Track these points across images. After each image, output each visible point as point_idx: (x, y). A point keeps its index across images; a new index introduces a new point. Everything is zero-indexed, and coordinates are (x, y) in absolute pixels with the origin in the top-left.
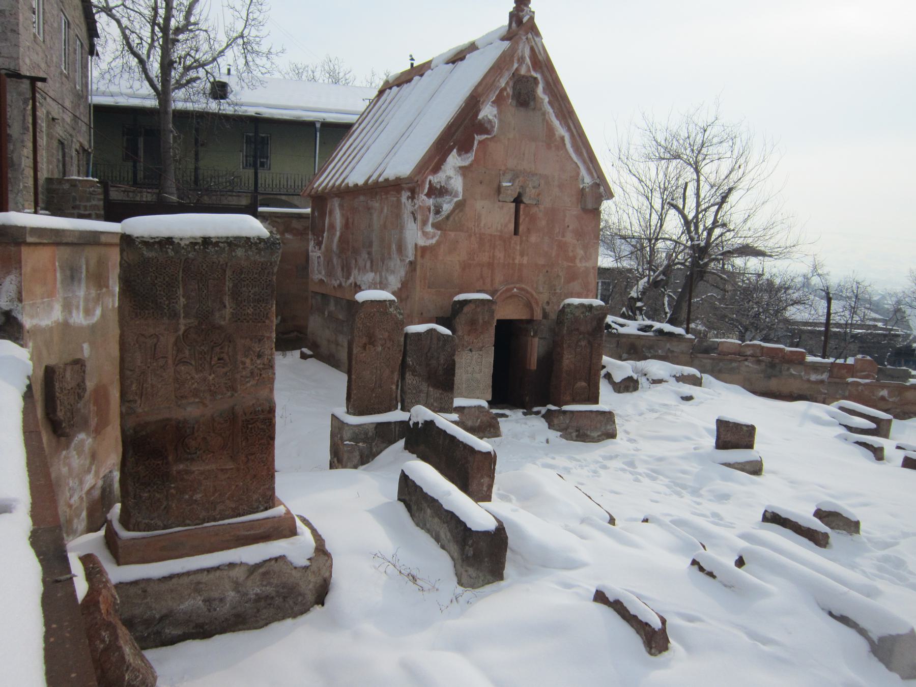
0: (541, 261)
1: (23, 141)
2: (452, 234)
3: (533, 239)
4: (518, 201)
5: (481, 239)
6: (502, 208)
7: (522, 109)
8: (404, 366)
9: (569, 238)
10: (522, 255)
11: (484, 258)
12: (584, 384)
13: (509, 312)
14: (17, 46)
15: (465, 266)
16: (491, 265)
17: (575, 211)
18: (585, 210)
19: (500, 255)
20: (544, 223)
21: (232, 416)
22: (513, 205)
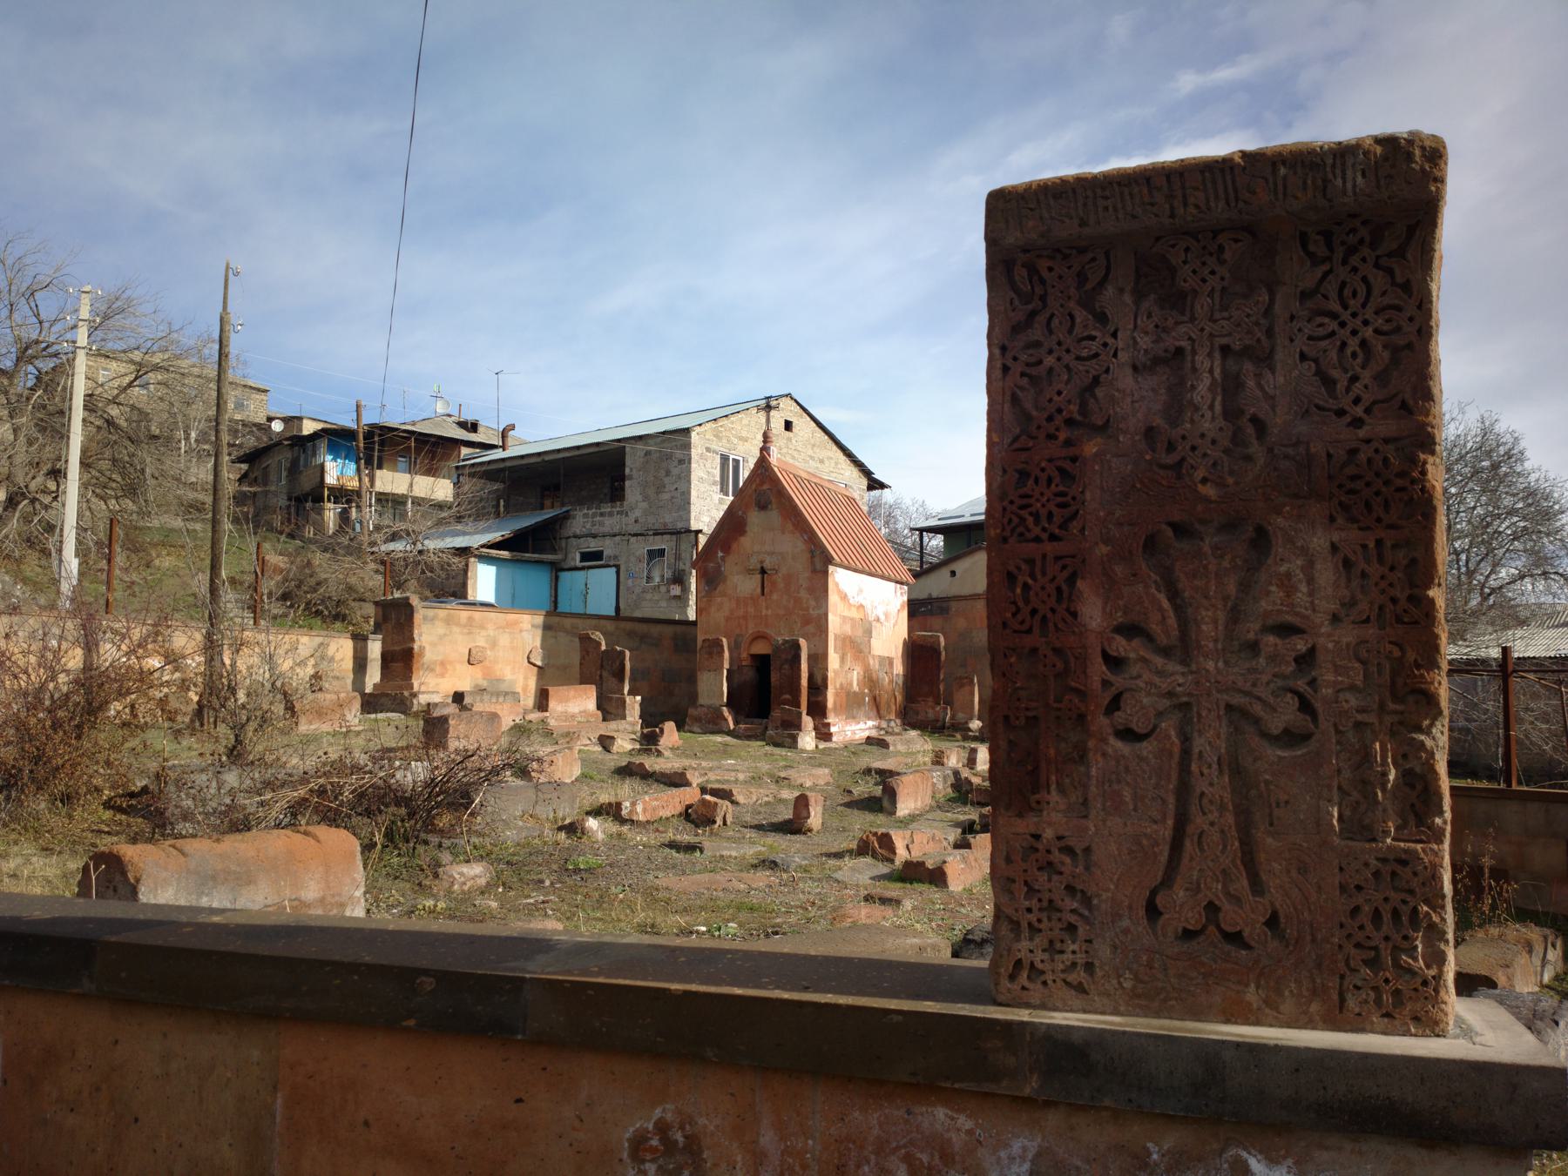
0: (782, 612)
1: (691, 573)
2: (719, 599)
3: (775, 597)
4: (763, 571)
5: (738, 600)
6: (751, 578)
7: (762, 512)
8: (602, 666)
9: (803, 594)
10: (767, 608)
11: (741, 612)
12: (788, 696)
13: (760, 648)
14: (689, 512)
15: (728, 619)
16: (745, 618)
17: (807, 574)
18: (814, 571)
19: (751, 610)
20: (782, 585)
21: (403, 649)
22: (759, 576)
